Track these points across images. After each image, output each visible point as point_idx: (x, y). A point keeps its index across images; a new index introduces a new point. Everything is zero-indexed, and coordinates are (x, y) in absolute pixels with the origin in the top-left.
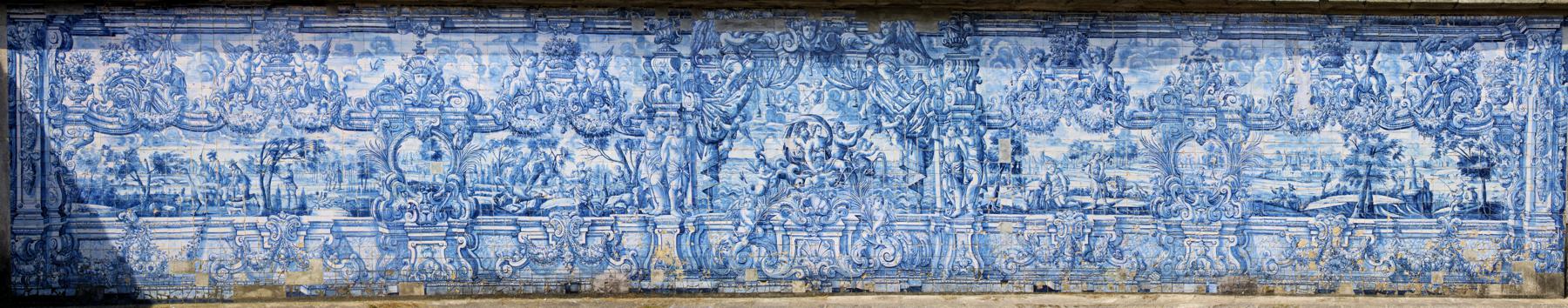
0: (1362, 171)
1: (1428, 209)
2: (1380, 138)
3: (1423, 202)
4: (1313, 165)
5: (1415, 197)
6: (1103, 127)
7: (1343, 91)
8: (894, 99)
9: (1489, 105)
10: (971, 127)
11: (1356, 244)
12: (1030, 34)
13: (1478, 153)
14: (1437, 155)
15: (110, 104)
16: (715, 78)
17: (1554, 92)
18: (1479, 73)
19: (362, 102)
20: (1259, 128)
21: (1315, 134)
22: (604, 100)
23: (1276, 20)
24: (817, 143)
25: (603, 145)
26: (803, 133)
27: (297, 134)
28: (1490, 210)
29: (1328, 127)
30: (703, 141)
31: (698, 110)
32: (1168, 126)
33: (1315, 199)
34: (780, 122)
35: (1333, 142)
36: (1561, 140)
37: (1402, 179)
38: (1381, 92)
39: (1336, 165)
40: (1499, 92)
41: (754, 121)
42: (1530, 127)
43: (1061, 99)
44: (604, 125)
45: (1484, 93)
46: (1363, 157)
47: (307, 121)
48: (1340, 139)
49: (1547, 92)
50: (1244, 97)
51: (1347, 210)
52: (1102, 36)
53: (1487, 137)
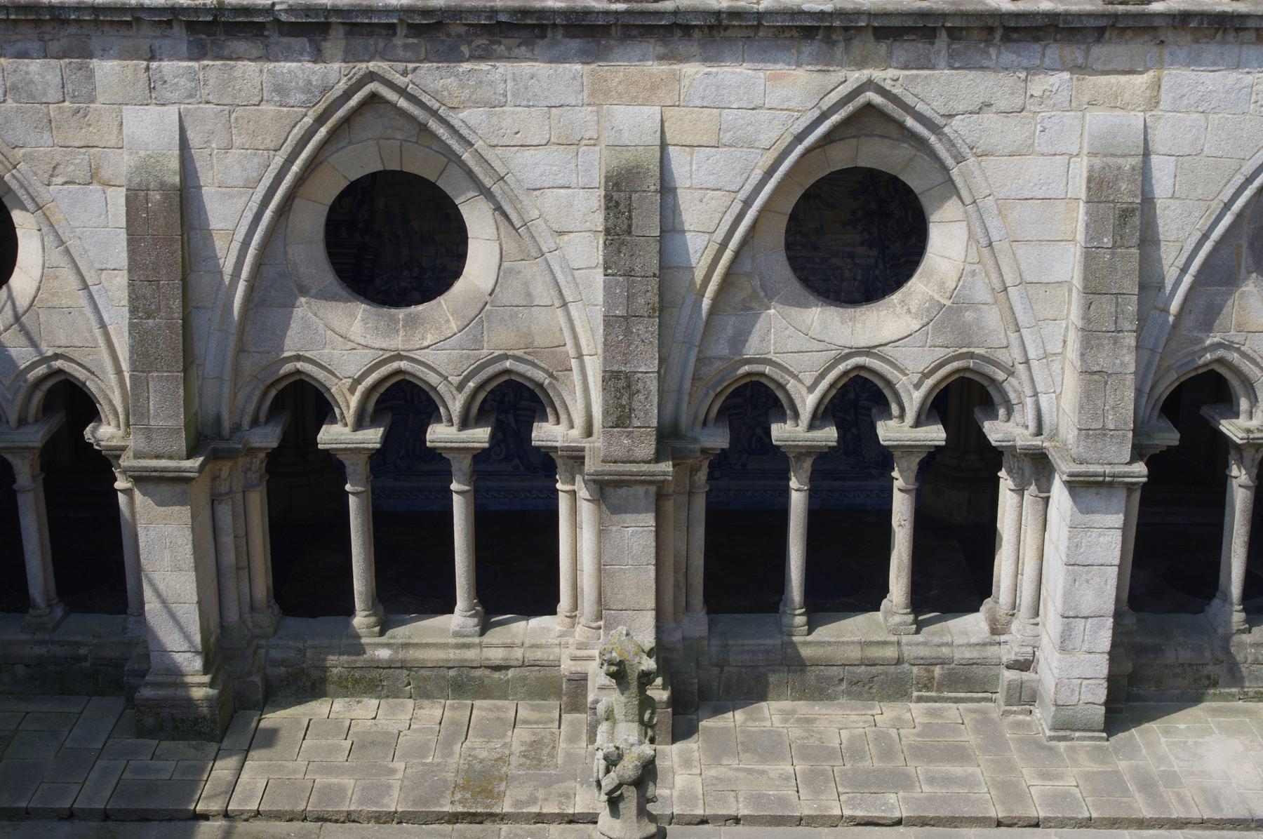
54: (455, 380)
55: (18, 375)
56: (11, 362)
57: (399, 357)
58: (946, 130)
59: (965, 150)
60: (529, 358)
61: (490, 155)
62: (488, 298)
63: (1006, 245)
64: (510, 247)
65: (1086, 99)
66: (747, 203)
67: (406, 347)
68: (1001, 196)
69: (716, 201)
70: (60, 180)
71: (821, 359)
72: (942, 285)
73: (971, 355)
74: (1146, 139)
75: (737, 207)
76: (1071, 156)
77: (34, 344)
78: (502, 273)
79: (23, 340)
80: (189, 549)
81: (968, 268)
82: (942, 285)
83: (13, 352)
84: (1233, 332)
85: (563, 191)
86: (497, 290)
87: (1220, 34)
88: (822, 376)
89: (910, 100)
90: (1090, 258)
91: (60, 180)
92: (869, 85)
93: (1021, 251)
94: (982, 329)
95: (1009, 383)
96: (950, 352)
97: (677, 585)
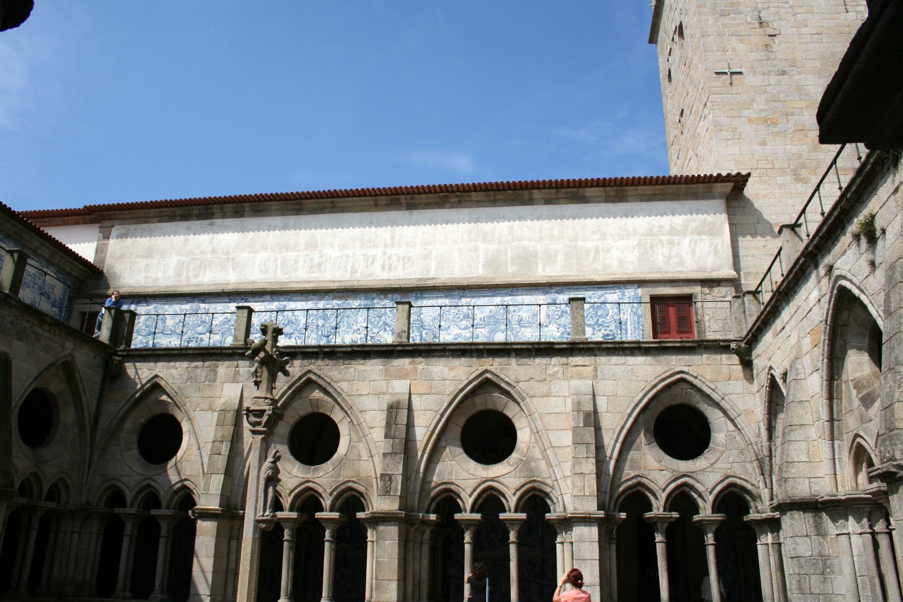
6: (466, 328)
7: (556, 313)
8: (391, 320)
10: (418, 329)
12: (441, 297)
13: (609, 333)
15: (144, 327)
16: (330, 315)
17: (637, 310)
19: (217, 325)
20: (525, 327)
21: (546, 328)
22: (292, 323)
23: (531, 289)
24: (363, 336)
25: (290, 338)
26: (358, 332)
27: (196, 336)
29: (551, 325)
30: (323, 336)
31: (323, 325)
32: (490, 327)
34: (351, 328)
36: (641, 327)
41: (342, 329)
42: (629, 323)
43: (451, 319)
44: (291, 331)
45: (610, 311)
47: (199, 331)
48: (556, 329)
49: (634, 310)
50: (519, 316)
52: (467, 297)
53: (612, 327)
54: (329, 491)
55: (170, 488)
56: (170, 481)
57: (308, 481)
58: (517, 388)
59: (525, 395)
60: (358, 481)
61: (347, 399)
62: (344, 457)
63: (543, 431)
64: (354, 436)
65: (569, 376)
66: (442, 415)
67: (313, 477)
68: (540, 412)
69: (430, 414)
70: (198, 409)
71: (474, 483)
72: (522, 453)
73: (535, 481)
74: (593, 389)
75: (438, 416)
76: (566, 397)
77: (179, 474)
78: (350, 447)
79: (175, 473)
80: (213, 547)
81: (532, 445)
82: (522, 453)
83: (171, 477)
84: (642, 470)
85: (373, 412)
86: (348, 453)
87: (616, 353)
88: (474, 490)
89: (503, 377)
90: (575, 429)
91: (198, 409)
92: (486, 371)
93: (550, 434)
94: (538, 470)
95: (553, 493)
96: (527, 480)
97: (414, 586)
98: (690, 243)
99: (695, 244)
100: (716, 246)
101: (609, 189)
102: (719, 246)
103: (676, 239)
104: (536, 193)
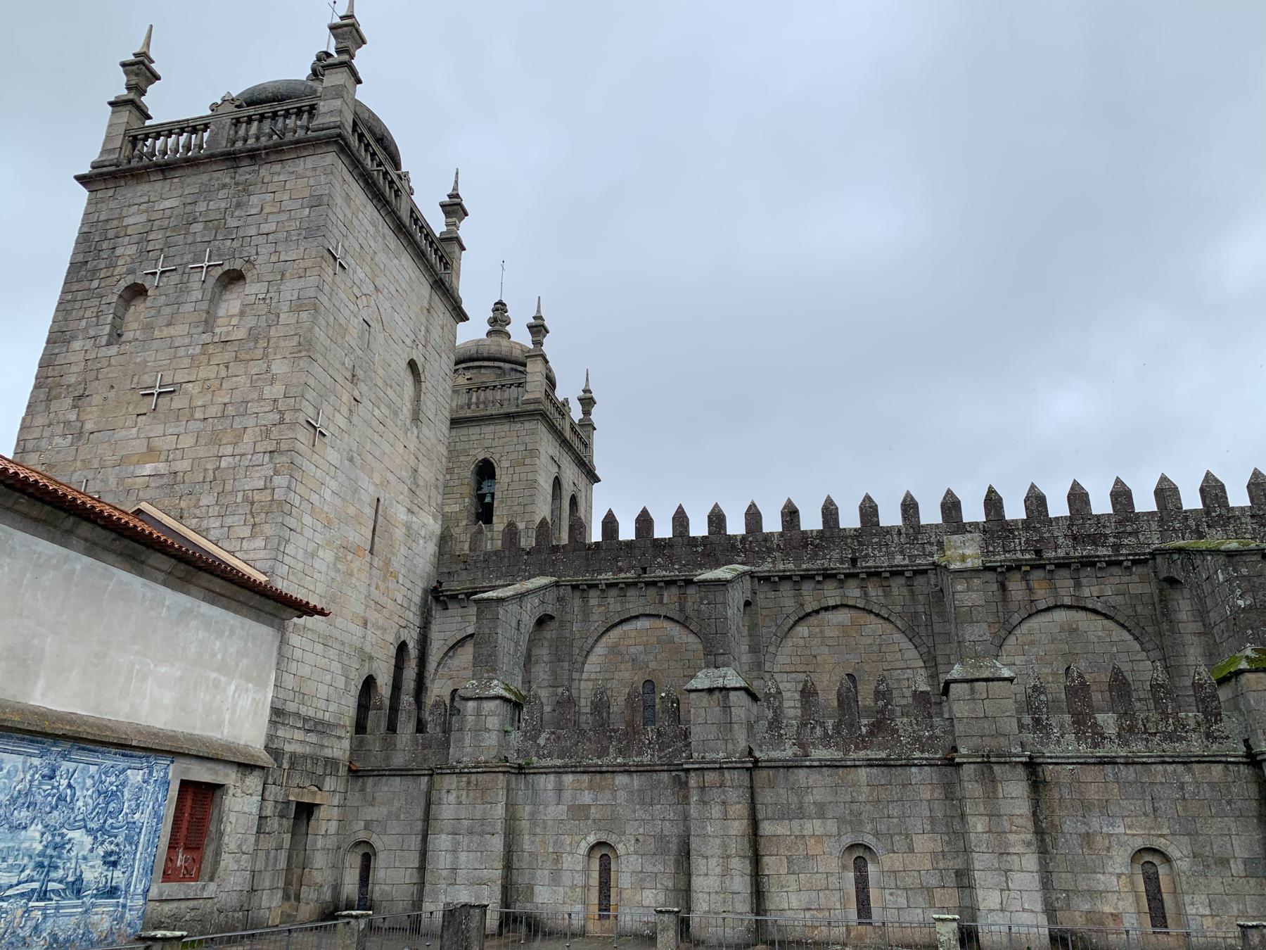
0: (46, 863)
1: (78, 893)
2: (63, 835)
3: (76, 888)
4: (16, 858)
5: (73, 883)
9: (127, 814)
11: (29, 923)
14: (92, 850)
18: (126, 790)
21: (23, 832)
28: (112, 892)
33: (11, 886)
35: (34, 838)
37: (69, 869)
38: (72, 801)
39: (30, 857)
40: (133, 806)
45: (126, 805)
46: (49, 851)
48: (38, 835)
51: (28, 896)
53: (121, 839)
98: (235, 692)
99: (239, 696)
100: (257, 704)
101: (182, 566)
102: (260, 705)
103: (223, 679)
104: (85, 529)
